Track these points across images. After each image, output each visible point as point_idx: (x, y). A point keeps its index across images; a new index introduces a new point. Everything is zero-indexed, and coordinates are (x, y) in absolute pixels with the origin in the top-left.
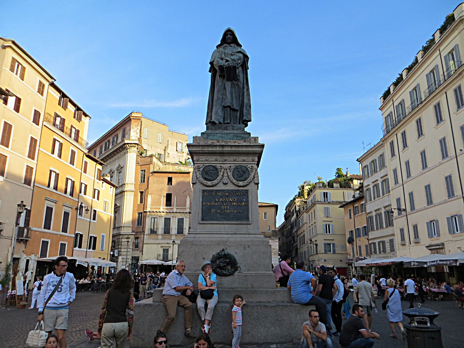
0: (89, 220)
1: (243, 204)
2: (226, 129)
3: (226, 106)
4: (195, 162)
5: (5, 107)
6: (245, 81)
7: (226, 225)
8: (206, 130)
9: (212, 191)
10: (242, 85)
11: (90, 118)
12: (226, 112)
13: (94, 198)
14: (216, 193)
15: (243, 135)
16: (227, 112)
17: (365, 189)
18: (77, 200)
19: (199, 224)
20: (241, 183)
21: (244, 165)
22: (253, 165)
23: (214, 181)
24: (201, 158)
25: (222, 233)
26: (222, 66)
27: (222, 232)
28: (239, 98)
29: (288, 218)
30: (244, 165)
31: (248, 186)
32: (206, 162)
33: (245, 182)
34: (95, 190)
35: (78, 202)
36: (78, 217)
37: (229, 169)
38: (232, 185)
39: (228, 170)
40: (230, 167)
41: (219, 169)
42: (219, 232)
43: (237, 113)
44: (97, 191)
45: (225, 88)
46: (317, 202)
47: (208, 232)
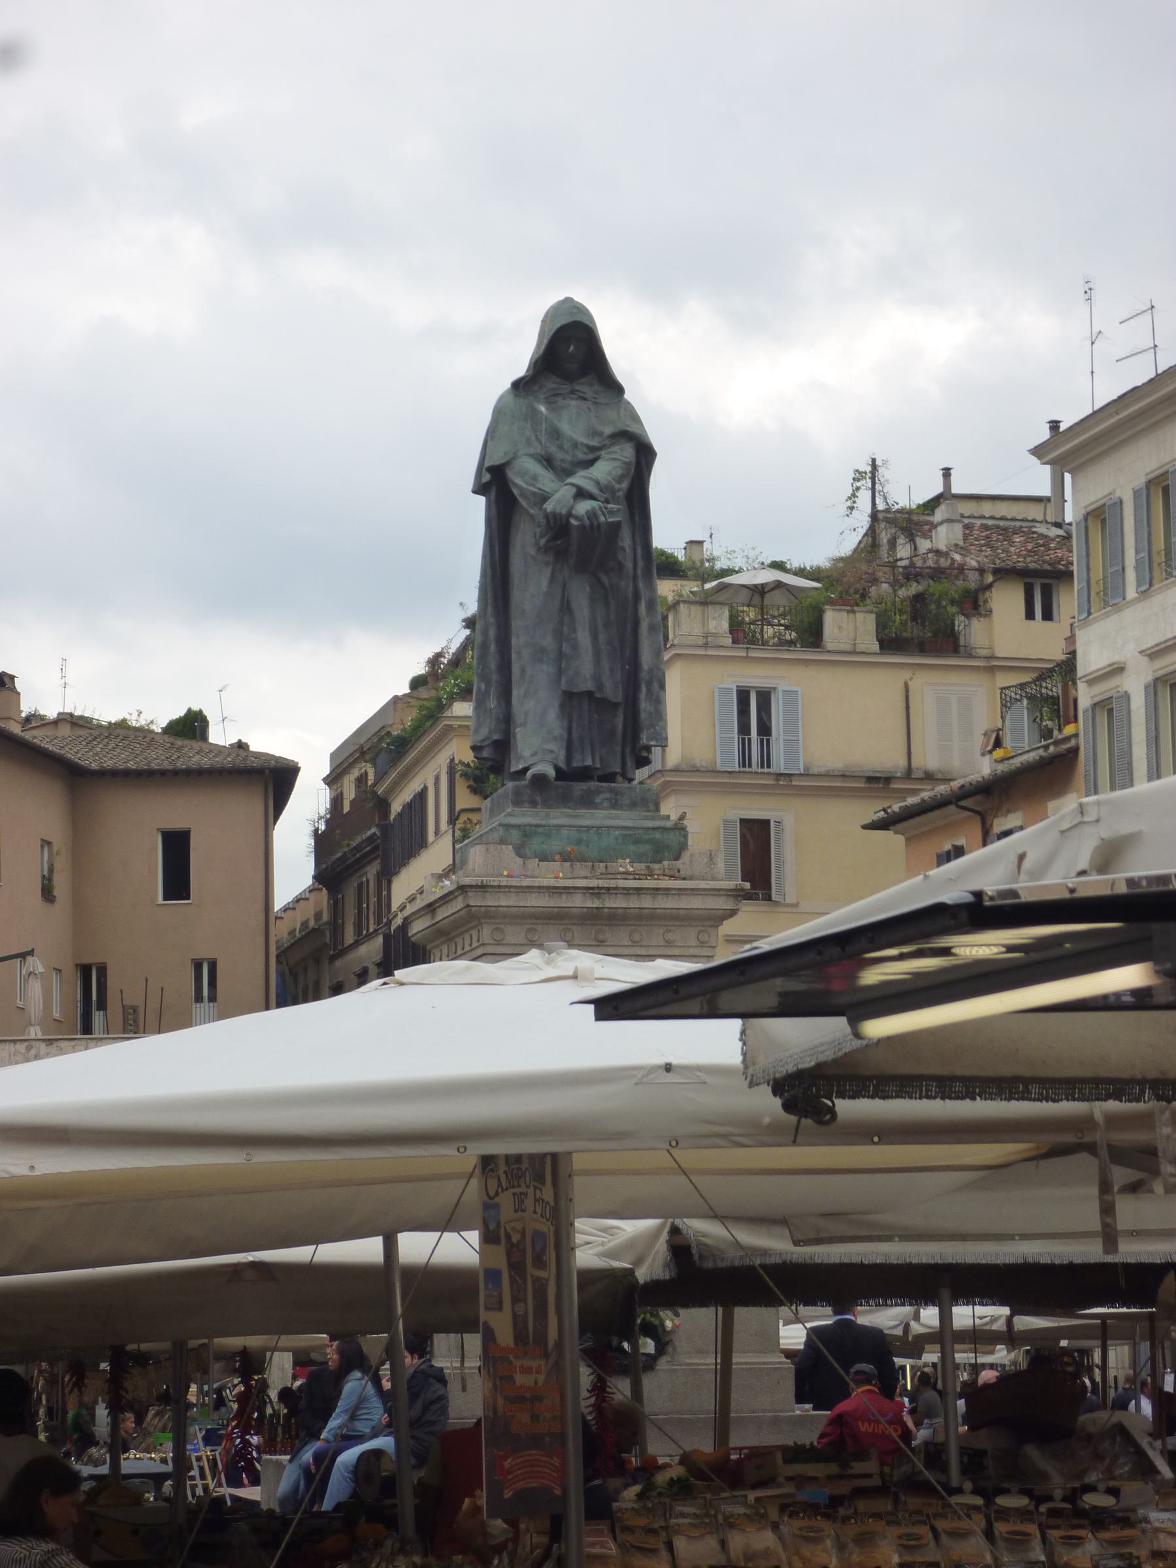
2: (587, 801)
6: (640, 563)
10: (631, 589)
15: (658, 835)
17: (1085, 697)
26: (560, 514)
29: (357, 863)
45: (566, 608)
46: (676, 770)
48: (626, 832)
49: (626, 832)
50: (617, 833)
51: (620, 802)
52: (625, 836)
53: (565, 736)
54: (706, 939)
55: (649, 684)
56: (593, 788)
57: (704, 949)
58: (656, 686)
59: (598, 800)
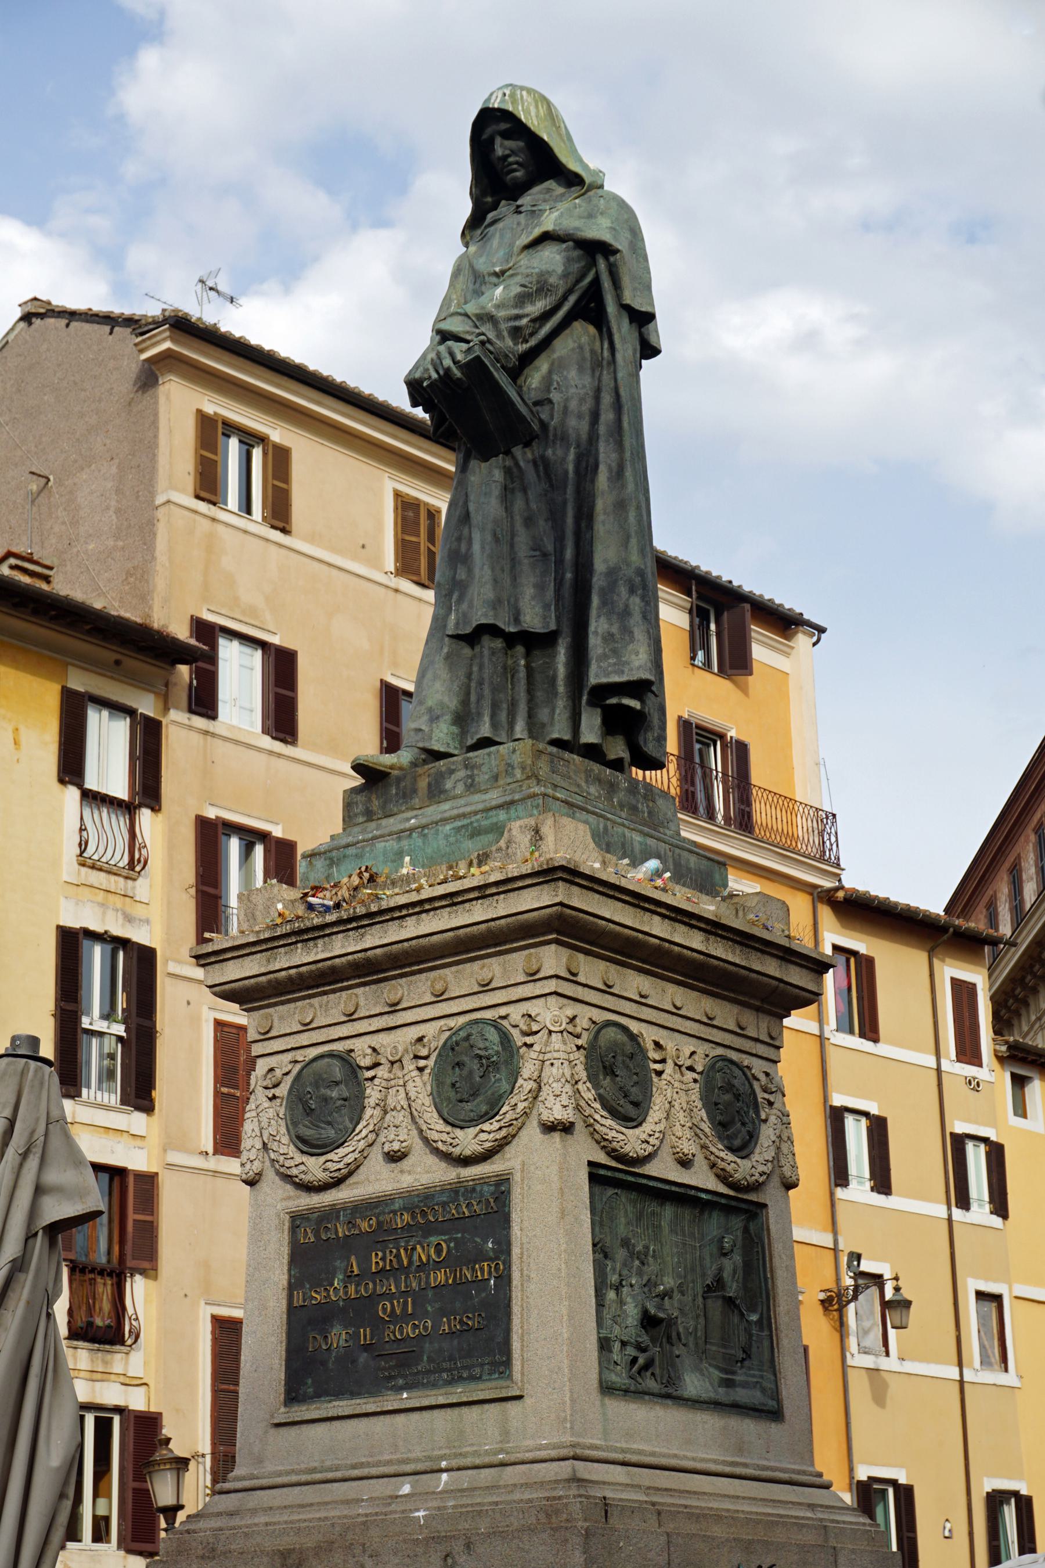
0: (953, 1373)
1: (482, 1269)
2: (436, 792)
3: (468, 630)
4: (257, 1049)
5: (206, 733)
7: (400, 1419)
8: (338, 827)
9: (332, 1213)
10: (571, 457)
11: (822, 630)
12: (475, 669)
13: (963, 1201)
14: (354, 1226)
16: (481, 667)
18: (827, 1240)
19: (273, 1431)
20: (468, 1141)
21: (488, 1014)
22: (533, 1008)
23: (341, 1151)
24: (281, 1018)
25: (374, 1471)
27: (378, 1464)
28: (560, 551)
30: (488, 1014)
31: (510, 1151)
32: (304, 1039)
33: (486, 1127)
34: (959, 1142)
35: (835, 1250)
36: (850, 1361)
37: (416, 1057)
38: (432, 1160)
39: (410, 1066)
40: (420, 1039)
41: (368, 1069)
42: (362, 1465)
43: (554, 656)
44: (976, 1158)
47: (314, 1470)
48: (459, 824)
49: (459, 824)
50: (448, 827)
51: (477, 779)
52: (458, 830)
53: (453, 703)
54: (535, 968)
55: (604, 594)
56: (443, 769)
57: (539, 984)
58: (623, 590)
59: (448, 785)
